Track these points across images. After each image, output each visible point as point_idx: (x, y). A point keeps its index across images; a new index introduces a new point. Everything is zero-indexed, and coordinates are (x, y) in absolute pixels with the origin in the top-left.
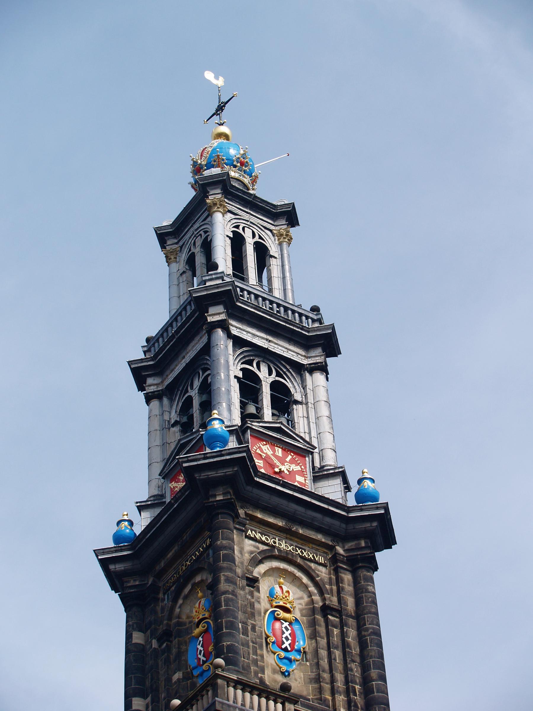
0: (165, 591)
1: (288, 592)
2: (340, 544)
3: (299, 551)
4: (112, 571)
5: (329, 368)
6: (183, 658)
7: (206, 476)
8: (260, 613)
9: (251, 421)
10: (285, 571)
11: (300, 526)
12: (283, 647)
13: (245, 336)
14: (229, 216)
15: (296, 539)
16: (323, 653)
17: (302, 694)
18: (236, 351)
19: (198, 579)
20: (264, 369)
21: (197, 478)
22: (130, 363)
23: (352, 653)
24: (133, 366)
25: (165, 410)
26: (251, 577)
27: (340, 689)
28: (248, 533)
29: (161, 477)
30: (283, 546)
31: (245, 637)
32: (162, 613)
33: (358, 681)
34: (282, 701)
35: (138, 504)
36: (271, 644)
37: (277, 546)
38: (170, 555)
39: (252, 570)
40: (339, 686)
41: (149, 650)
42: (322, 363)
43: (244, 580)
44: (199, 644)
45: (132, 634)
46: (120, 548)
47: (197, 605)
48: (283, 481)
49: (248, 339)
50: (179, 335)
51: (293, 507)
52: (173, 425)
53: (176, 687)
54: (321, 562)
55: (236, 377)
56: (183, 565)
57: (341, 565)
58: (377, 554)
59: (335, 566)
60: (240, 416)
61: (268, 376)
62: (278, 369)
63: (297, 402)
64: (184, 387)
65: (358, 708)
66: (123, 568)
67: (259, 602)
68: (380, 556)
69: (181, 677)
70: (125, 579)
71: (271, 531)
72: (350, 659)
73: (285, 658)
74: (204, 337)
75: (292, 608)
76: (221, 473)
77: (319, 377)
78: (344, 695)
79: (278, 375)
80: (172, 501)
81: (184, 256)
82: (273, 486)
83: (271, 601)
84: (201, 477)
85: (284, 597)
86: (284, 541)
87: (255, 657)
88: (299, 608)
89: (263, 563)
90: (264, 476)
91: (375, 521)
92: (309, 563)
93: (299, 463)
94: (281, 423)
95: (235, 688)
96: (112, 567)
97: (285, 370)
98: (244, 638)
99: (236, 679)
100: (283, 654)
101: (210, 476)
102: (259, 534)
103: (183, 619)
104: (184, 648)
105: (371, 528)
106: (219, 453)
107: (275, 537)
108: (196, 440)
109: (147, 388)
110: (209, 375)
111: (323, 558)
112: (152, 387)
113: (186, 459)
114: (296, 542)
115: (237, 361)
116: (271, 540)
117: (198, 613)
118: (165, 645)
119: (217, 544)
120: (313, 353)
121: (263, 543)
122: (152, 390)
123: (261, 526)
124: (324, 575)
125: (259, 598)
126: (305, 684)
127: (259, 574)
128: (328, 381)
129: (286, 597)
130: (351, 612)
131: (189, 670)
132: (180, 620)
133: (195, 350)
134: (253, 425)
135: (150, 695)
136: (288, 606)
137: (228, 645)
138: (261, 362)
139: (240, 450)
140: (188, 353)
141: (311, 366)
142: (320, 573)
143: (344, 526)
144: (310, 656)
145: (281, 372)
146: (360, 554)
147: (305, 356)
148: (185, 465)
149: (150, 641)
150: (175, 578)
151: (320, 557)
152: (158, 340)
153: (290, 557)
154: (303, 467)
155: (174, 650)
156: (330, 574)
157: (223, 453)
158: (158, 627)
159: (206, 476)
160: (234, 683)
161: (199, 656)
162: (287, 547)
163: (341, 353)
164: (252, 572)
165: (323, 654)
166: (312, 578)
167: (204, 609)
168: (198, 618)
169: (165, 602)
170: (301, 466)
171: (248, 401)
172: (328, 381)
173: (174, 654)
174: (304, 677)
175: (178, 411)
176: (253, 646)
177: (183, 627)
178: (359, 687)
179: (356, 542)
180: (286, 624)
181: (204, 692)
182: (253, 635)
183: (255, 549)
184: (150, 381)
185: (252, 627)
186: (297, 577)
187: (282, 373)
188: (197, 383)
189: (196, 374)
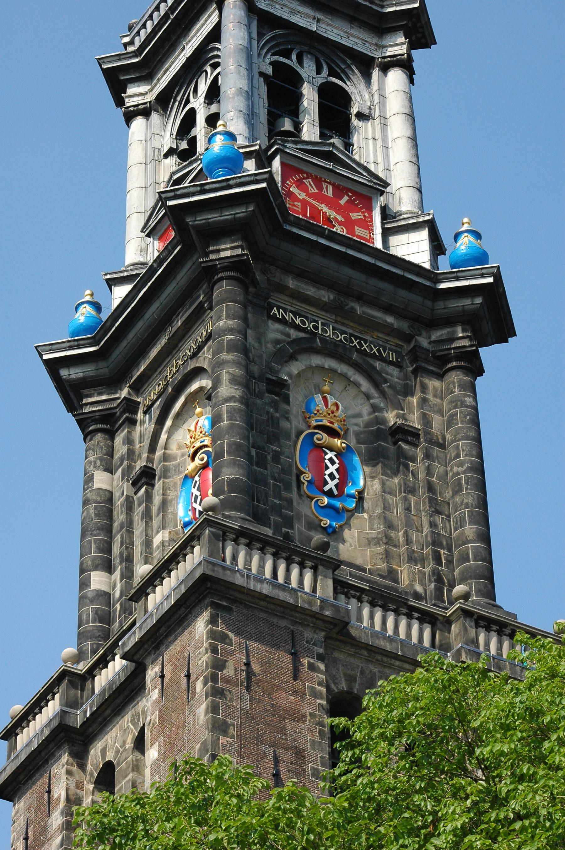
0: (145, 409)
1: (337, 405)
2: (424, 333)
3: (355, 343)
4: (65, 379)
5: (416, 65)
6: (170, 510)
7: (204, 221)
8: (288, 437)
9: (282, 140)
10: (333, 371)
11: (359, 303)
12: (326, 488)
13: (279, 11)
15: (352, 324)
17: (352, 562)
18: (264, 35)
19: (195, 386)
21: (190, 223)
22: (100, 61)
23: (437, 499)
24: (105, 67)
25: (155, 132)
26: (274, 378)
27: (416, 555)
28: (273, 311)
29: (143, 235)
30: (330, 333)
31: (261, 470)
32: (140, 442)
33: (445, 543)
34: (313, 564)
35: (108, 277)
36: (306, 483)
37: (320, 333)
39: (276, 369)
40: (414, 551)
41: (119, 500)
42: (403, 55)
43: (263, 382)
44: (194, 487)
45: (93, 475)
46: (76, 343)
47: (192, 428)
48: (329, 231)
49: (284, 17)
50: (175, 14)
51: (347, 272)
52: (166, 156)
53: (158, 553)
54: (391, 359)
55: (261, 74)
56: (173, 366)
57: (423, 365)
58: (483, 351)
59: (414, 366)
60: (267, 135)
61: (315, 76)
62: (333, 65)
63: (361, 116)
64: (184, 95)
65: (443, 583)
66: (81, 375)
67: (288, 419)
69: (167, 539)
70: (85, 392)
71: (309, 310)
72: (433, 509)
73: (329, 506)
74: (215, 14)
75: (342, 430)
76: (227, 215)
78: (421, 565)
79: (332, 73)
80: (155, 265)
82: (314, 238)
84: (196, 223)
85: (330, 412)
86: (331, 326)
87: (277, 501)
88: (354, 432)
89: (297, 360)
90: (298, 223)
91: (478, 296)
92: (371, 361)
93: (361, 208)
94: (333, 145)
95: (236, 541)
96: (64, 373)
97: (343, 67)
98: (259, 471)
99: (238, 528)
100: (326, 500)
101: (210, 220)
102: (290, 314)
103: (172, 450)
104: (171, 494)
105: (473, 307)
106: (224, 184)
107: (317, 319)
108: (197, 171)
109: (127, 100)
110: (219, 73)
111: (394, 354)
112: (135, 99)
113: (172, 194)
114: (352, 328)
115: (265, 50)
116: (309, 325)
117: (194, 438)
118: (143, 490)
119: (219, 325)
120: (388, 40)
121: (297, 328)
122: (136, 103)
123: (295, 302)
124: (396, 380)
125: (287, 412)
126: (360, 547)
127: (290, 376)
128: (413, 85)
129: (333, 412)
130: (437, 437)
131: (179, 527)
132: (168, 452)
133: (201, 36)
134: (286, 147)
135: (119, 567)
136: (336, 426)
137: (230, 480)
138: (304, 54)
139: (258, 177)
140: (190, 41)
141: (386, 60)
142: (390, 377)
143: (429, 303)
144: (370, 503)
145: (338, 70)
146: (455, 348)
147: (376, 45)
148: (170, 203)
149: (122, 485)
150: (160, 387)
151: (390, 353)
152: (144, 26)
153: (340, 350)
154: (366, 214)
155: (157, 497)
156: (406, 378)
157: (231, 182)
158: (133, 464)
159: (204, 221)
160: (235, 534)
161: (195, 505)
162: (336, 336)
163: (436, 43)
164: (278, 372)
165: (391, 502)
166: (376, 385)
167: (203, 433)
168: (193, 448)
169: (145, 425)
170: (363, 213)
171: (282, 112)
172: (413, 85)
173: (157, 504)
174: (358, 537)
175: (175, 133)
176: (274, 485)
177: (172, 463)
178: (446, 552)
179: (449, 330)
180: (330, 455)
181: (188, 550)
182: (276, 468)
183: (284, 337)
184: (132, 90)
185: (273, 455)
186: (353, 382)
187: (339, 71)
188: (203, 87)
189: (203, 72)
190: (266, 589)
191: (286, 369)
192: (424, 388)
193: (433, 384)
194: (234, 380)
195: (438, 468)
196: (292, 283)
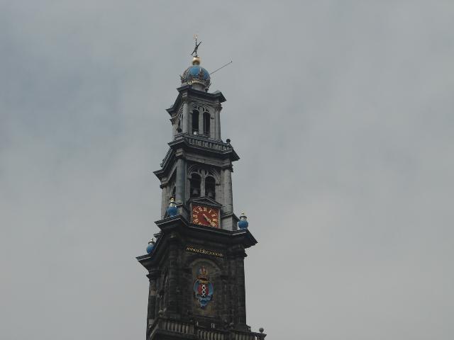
5: (233, 167)
14: (193, 103)
16: (220, 296)
20: (203, 172)
38: (163, 258)
63: (217, 185)
68: (247, 251)
76: (171, 227)
77: (227, 172)
81: (177, 122)
83: (197, 277)
90: (192, 225)
95: (167, 322)
100: (202, 299)
166: (216, 264)
180: (204, 286)
190: (173, 334)
191: (191, 264)
192: (230, 263)
193: (232, 261)
194: (172, 273)
195: (232, 286)
196: (192, 240)
